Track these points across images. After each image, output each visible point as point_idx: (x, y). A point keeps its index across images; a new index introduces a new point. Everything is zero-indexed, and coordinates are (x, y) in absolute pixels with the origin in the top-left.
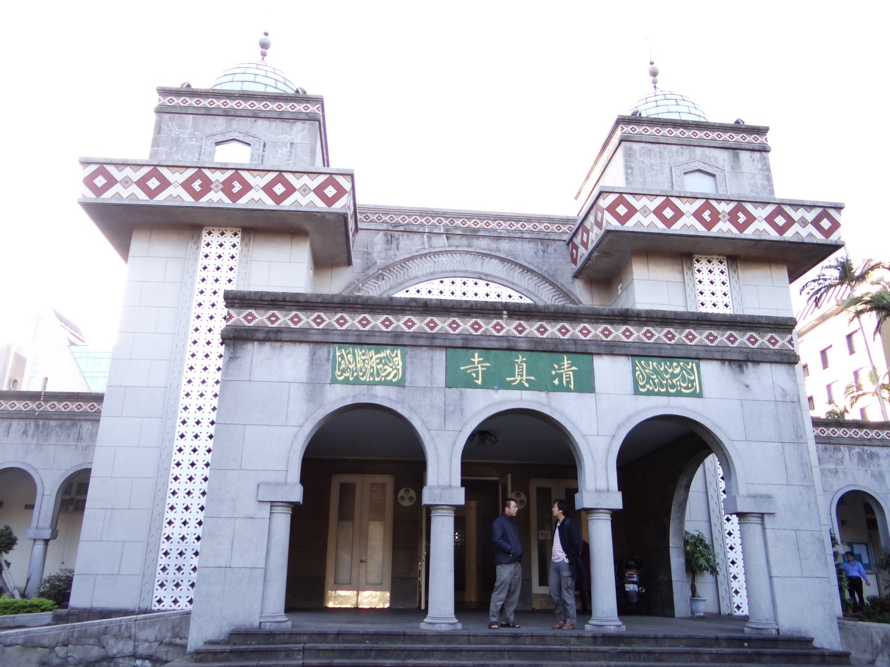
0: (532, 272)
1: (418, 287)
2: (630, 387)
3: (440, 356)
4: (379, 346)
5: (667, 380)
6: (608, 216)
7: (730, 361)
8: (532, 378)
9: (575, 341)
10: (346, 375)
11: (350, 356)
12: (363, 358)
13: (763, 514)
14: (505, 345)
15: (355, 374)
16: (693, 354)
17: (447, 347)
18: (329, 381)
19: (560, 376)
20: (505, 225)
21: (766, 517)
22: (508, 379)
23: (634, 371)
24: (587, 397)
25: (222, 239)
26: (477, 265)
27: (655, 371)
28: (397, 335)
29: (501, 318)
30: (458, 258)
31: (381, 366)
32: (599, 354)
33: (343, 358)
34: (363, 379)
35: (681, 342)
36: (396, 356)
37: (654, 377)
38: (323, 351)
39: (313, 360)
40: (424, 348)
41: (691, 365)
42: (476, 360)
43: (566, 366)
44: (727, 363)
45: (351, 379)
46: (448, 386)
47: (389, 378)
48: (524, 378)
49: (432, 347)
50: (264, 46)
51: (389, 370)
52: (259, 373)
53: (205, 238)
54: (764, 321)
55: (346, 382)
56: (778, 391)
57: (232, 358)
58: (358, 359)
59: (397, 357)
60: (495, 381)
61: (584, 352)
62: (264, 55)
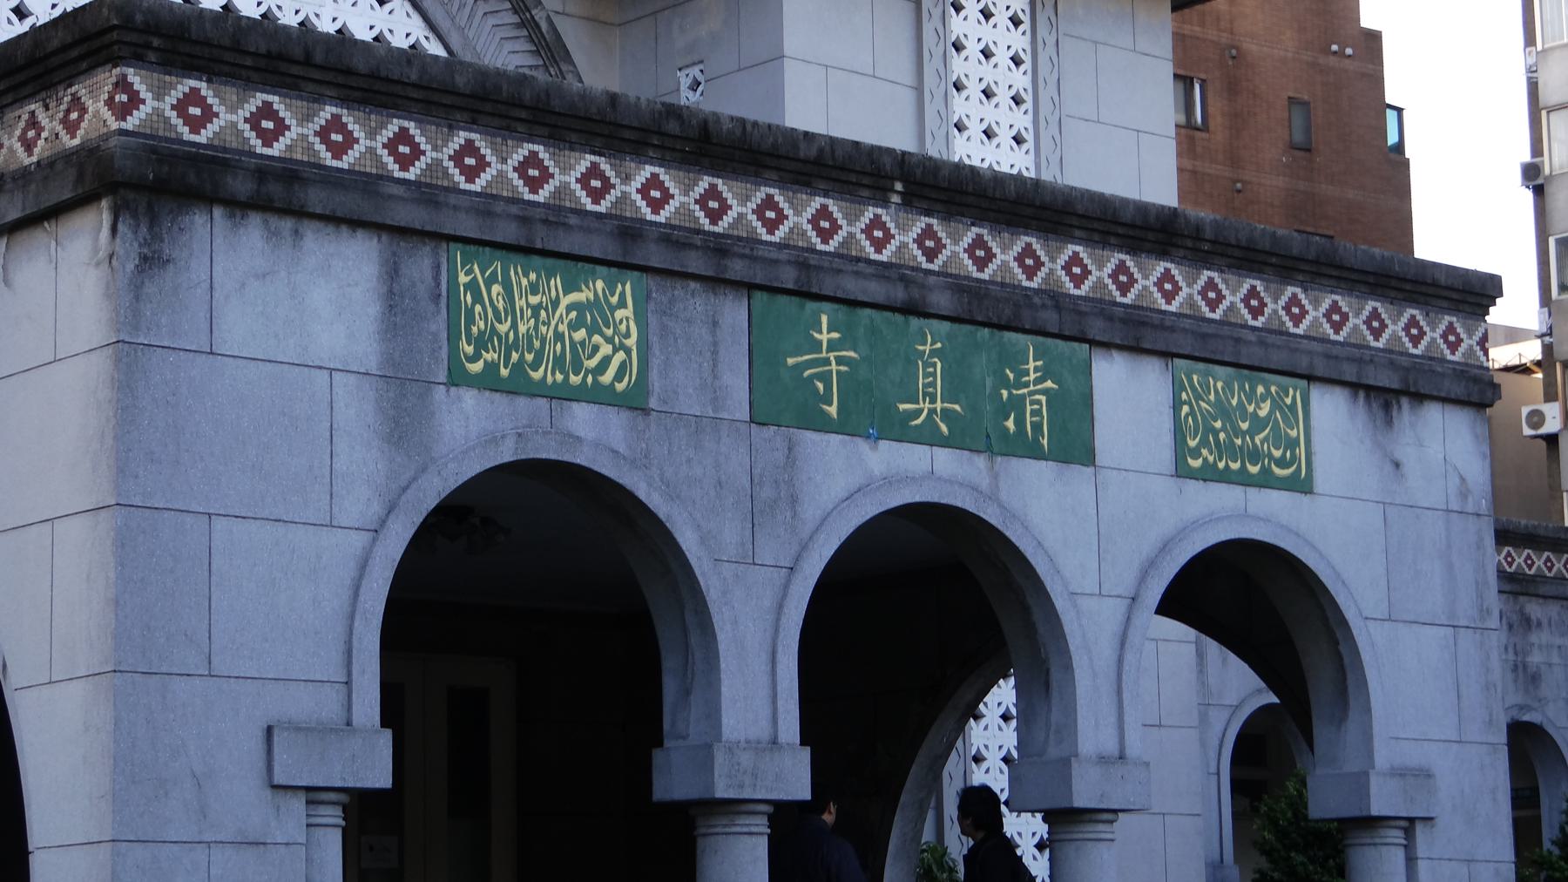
2: (1166, 455)
3: (734, 312)
4: (577, 262)
5: (1243, 434)
7: (1370, 389)
8: (957, 407)
9: (1055, 298)
10: (490, 356)
11: (496, 288)
12: (534, 300)
13: (1411, 820)
14: (899, 294)
15: (515, 356)
16: (1303, 364)
17: (750, 287)
18: (442, 378)
19: (1017, 405)
21: (1419, 827)
22: (902, 407)
23: (1177, 405)
24: (1080, 475)
27: (1223, 410)
28: (629, 230)
29: (885, 203)
31: (580, 334)
32: (1107, 346)
33: (478, 298)
34: (537, 375)
35: (1275, 325)
36: (622, 304)
37: (1218, 424)
38: (419, 265)
39: (395, 303)
40: (693, 285)
41: (1293, 395)
42: (824, 337)
43: (1032, 376)
44: (1362, 394)
45: (504, 372)
46: (757, 419)
47: (607, 378)
48: (939, 406)
49: (716, 282)
51: (606, 349)
52: (240, 328)
54: (1443, 280)
55: (489, 382)
56: (1454, 482)
57: (151, 261)
58: (520, 303)
59: (623, 302)
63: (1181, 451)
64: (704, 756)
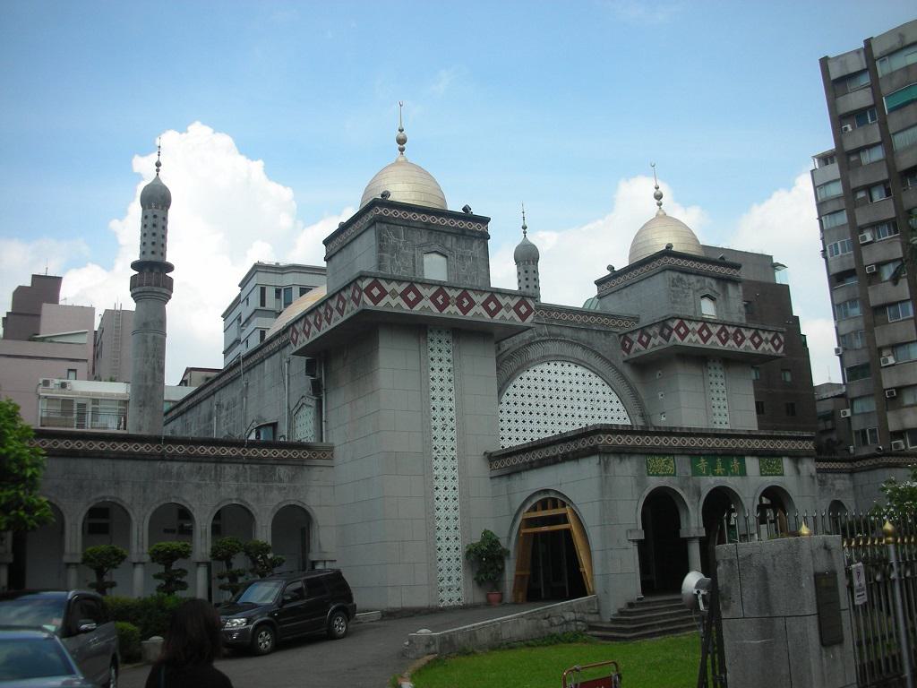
0: (600, 356)
1: (535, 368)
4: (665, 455)
6: (675, 335)
25: (440, 337)
26: (568, 351)
30: (557, 344)
41: (780, 459)
46: (693, 475)
50: (401, 141)
53: (430, 335)
55: (653, 475)
60: (711, 471)
61: (741, 455)
62: (402, 150)
63: (761, 472)
64: (688, 530)
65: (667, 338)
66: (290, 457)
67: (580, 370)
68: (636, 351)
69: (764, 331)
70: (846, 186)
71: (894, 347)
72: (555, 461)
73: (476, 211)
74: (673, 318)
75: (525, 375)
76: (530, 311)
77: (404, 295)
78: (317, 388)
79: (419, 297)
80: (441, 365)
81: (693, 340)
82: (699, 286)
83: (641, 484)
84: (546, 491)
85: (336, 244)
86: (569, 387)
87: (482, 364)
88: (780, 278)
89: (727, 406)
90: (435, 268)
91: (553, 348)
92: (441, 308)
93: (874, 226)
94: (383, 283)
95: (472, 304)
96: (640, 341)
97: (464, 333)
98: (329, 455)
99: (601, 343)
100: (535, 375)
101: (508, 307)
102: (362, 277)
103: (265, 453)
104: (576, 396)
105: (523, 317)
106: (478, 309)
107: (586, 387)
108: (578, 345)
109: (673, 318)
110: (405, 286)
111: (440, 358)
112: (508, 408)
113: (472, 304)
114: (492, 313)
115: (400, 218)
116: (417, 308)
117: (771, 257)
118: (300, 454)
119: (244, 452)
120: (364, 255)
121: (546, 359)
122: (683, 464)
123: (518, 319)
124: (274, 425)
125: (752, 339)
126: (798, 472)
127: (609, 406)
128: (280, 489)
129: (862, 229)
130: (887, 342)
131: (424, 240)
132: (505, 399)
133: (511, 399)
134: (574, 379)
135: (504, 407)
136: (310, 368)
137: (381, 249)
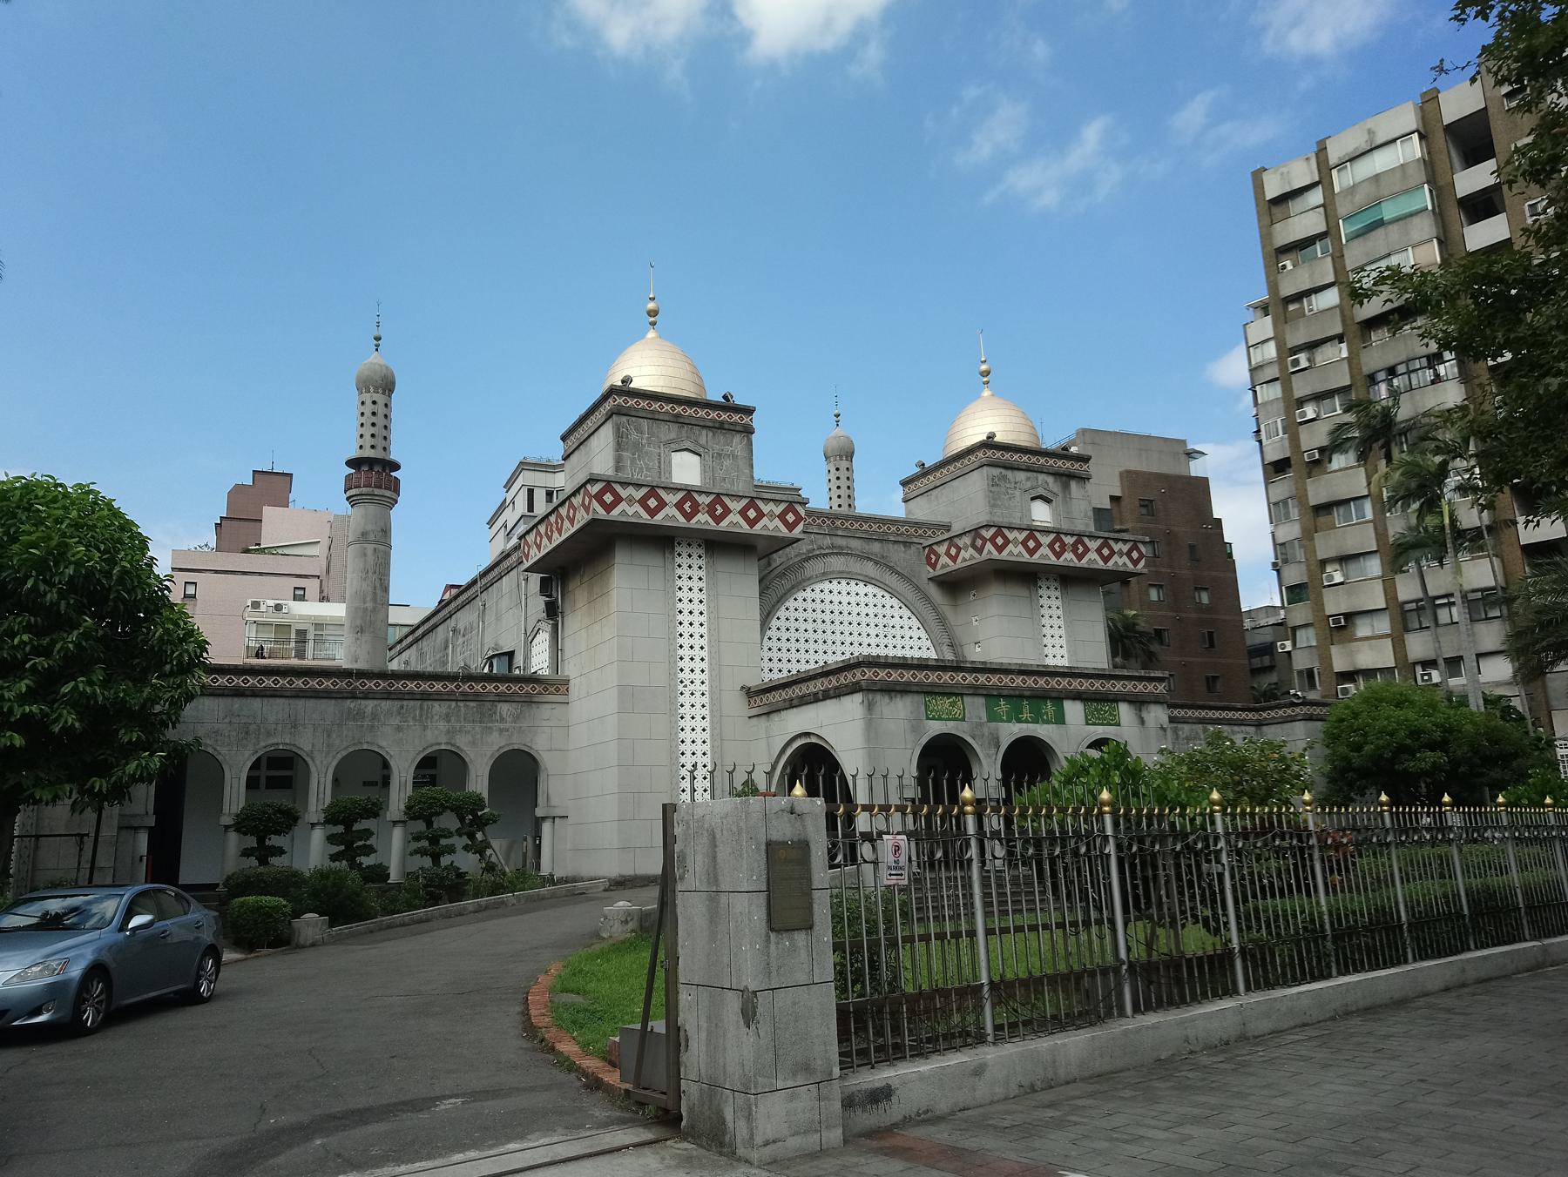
6: (989, 546)
20: (875, 527)
25: (690, 551)
26: (856, 566)
30: (842, 559)
53: (678, 549)
65: (980, 551)
66: (515, 693)
67: (870, 589)
68: (944, 566)
69: (1117, 540)
70: (1279, 348)
71: (1344, 560)
72: (816, 699)
73: (739, 400)
74: (988, 526)
75: (800, 595)
76: (799, 519)
77: (643, 502)
78: (552, 611)
79: (662, 504)
80: (690, 583)
81: (1015, 553)
82: (1029, 484)
83: (916, 729)
84: (807, 734)
85: (573, 440)
86: (855, 610)
87: (743, 583)
88: (1196, 469)
89: (1063, 636)
90: (686, 469)
91: (837, 563)
92: (688, 517)
93: (1318, 397)
94: (618, 488)
95: (727, 511)
96: (948, 554)
97: (719, 546)
98: (563, 689)
99: (898, 555)
100: (813, 595)
101: (771, 515)
102: (592, 480)
103: (484, 688)
104: (864, 620)
105: (791, 527)
106: (735, 518)
107: (879, 610)
108: (869, 559)
109: (988, 526)
110: (644, 491)
111: (691, 577)
112: (779, 634)
113: (727, 511)
114: (752, 523)
115: (643, 409)
116: (659, 517)
117: (1184, 442)
118: (528, 688)
119: (458, 687)
120: (600, 456)
121: (827, 576)
122: (975, 707)
123: (784, 529)
124: (511, 655)
125: (1099, 551)
126: (1142, 722)
127: (908, 634)
128: (501, 730)
129: (1301, 402)
130: (1332, 554)
131: (673, 435)
132: (774, 623)
133: (782, 624)
134: (863, 600)
135: (772, 633)
136: (545, 587)
137: (619, 446)
